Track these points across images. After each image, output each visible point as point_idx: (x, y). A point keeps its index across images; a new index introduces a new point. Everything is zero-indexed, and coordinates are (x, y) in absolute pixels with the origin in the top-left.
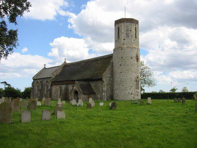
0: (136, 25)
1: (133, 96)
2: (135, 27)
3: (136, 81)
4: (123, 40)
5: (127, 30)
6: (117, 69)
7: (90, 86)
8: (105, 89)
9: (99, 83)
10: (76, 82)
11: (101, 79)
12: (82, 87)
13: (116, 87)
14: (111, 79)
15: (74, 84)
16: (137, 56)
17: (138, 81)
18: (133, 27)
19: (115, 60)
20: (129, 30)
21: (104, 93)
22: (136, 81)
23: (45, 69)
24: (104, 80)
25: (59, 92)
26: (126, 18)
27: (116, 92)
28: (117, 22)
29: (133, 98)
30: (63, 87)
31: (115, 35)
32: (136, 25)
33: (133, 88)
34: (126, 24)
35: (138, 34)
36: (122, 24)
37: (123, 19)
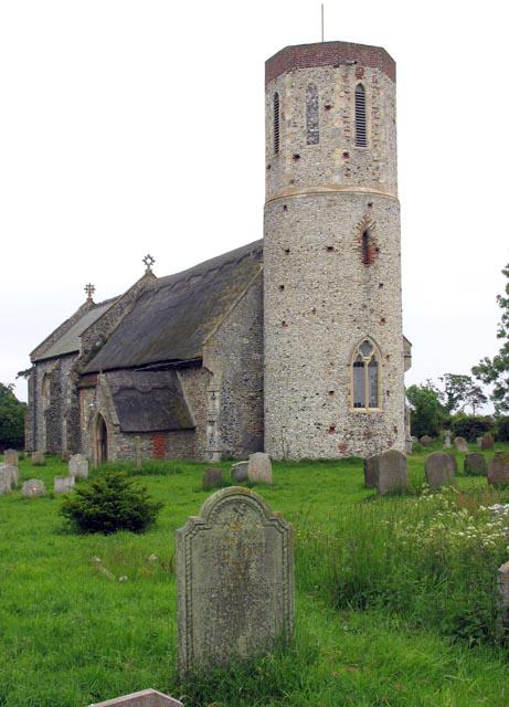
0: (359, 76)
1: (338, 438)
2: (354, 83)
3: (359, 364)
4: (289, 161)
5: (312, 108)
7: (174, 391)
9: (200, 380)
10: (102, 378)
11: (197, 364)
12: (127, 403)
14: (256, 356)
15: (94, 387)
17: (374, 364)
20: (321, 103)
21: (209, 429)
22: (359, 364)
24: (209, 363)
26: (326, 40)
27: (272, 419)
29: (343, 447)
32: (359, 76)
33: (341, 397)
34: (308, 75)
37: (338, 42)
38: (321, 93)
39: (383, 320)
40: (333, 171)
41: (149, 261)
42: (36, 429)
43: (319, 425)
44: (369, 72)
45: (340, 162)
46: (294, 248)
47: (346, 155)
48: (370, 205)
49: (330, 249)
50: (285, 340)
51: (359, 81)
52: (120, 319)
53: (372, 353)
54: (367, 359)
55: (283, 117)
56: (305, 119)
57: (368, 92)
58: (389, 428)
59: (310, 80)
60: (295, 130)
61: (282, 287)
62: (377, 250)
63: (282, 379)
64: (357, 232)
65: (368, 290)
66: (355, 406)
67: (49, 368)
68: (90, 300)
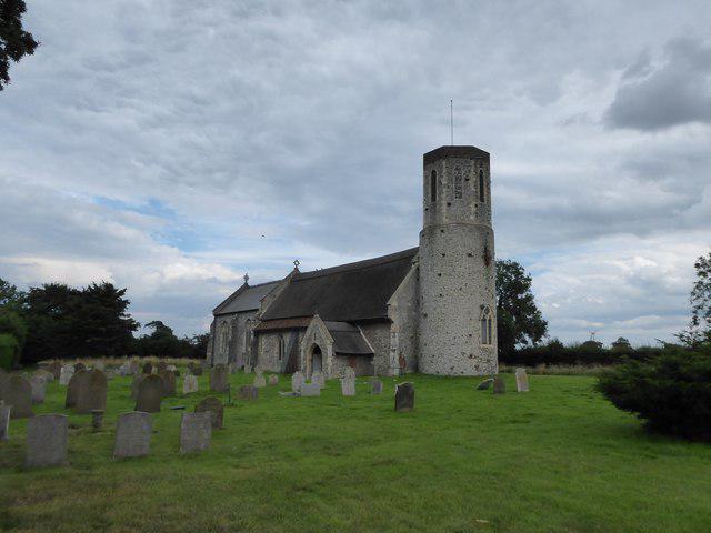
1: (474, 362)
4: (444, 207)
6: (430, 290)
8: (395, 341)
13: (424, 339)
16: (486, 250)
19: (423, 262)
21: (392, 354)
23: (246, 287)
24: (392, 315)
25: (277, 350)
28: (432, 158)
30: (287, 338)
31: (426, 194)
35: (489, 189)
36: (444, 163)
43: (463, 354)
45: (474, 209)
49: (470, 255)
67: (228, 319)
68: (246, 284)
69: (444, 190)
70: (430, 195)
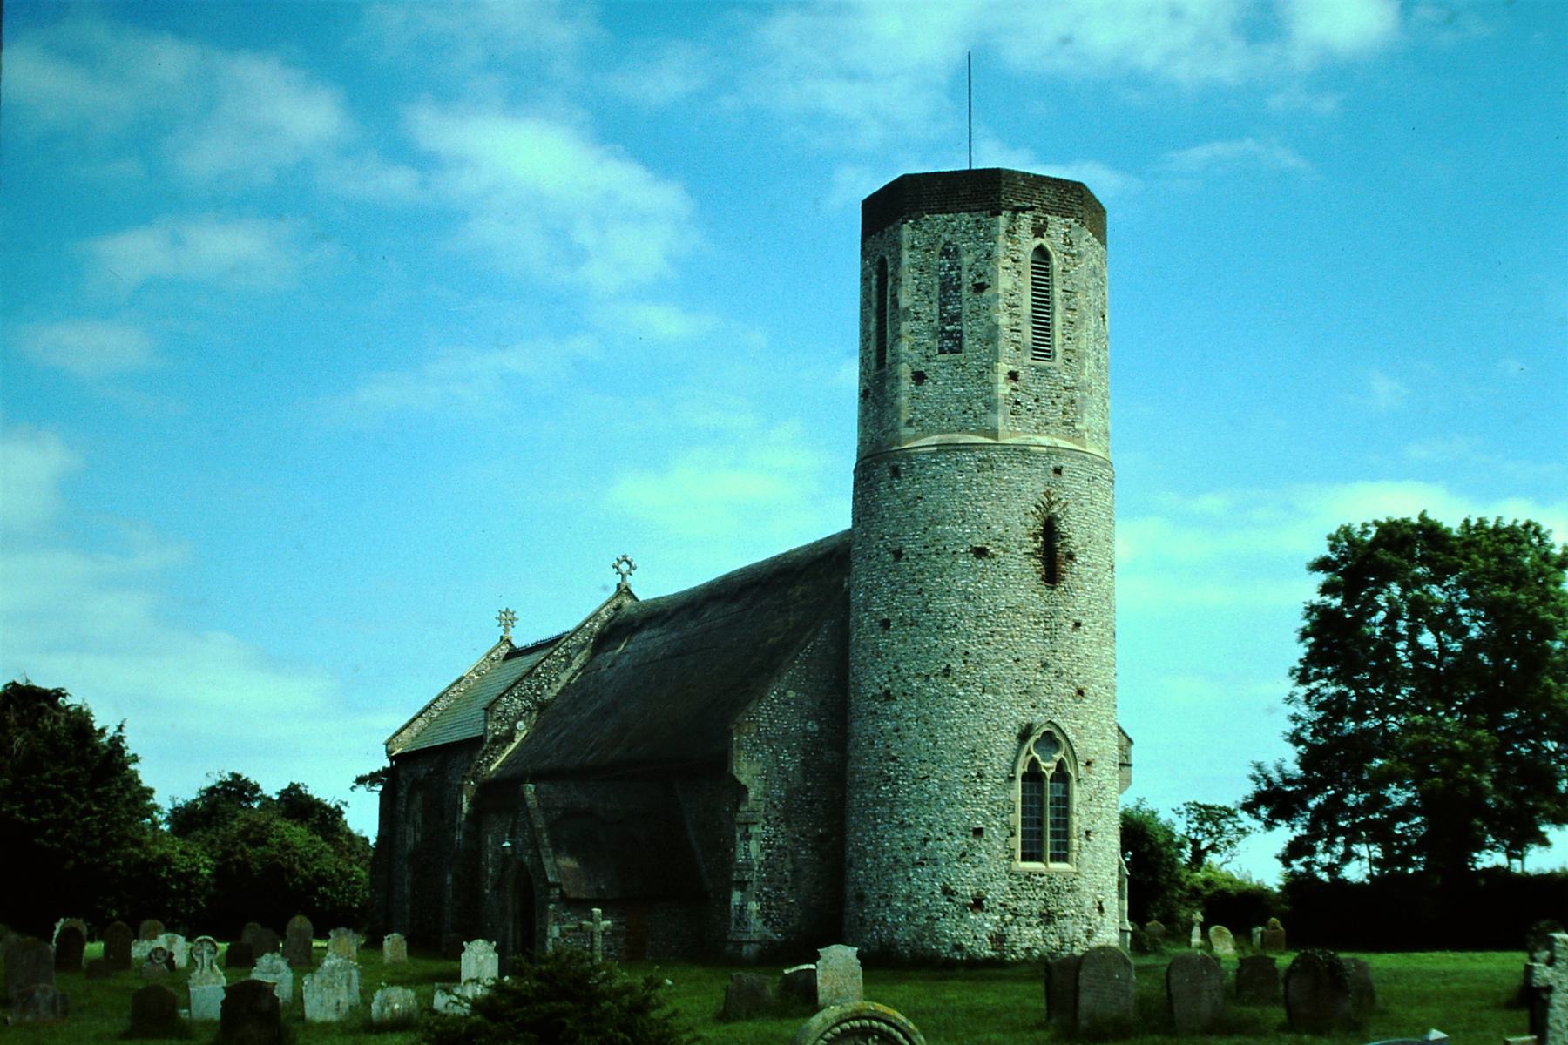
0: (1039, 231)
1: (988, 922)
2: (1029, 244)
3: (1033, 776)
4: (906, 384)
5: (949, 287)
14: (829, 755)
17: (1061, 775)
18: (1000, 252)
19: (861, 579)
20: (967, 278)
21: (736, 897)
22: (1033, 776)
31: (865, 340)
32: (1039, 231)
33: (995, 839)
38: (967, 260)
39: (1080, 692)
40: (988, 405)
41: (624, 567)
42: (531, 825)
44: (1057, 225)
46: (910, 547)
47: (1013, 376)
48: (1058, 471)
50: (889, 725)
51: (1039, 241)
52: (564, 677)
53: (1058, 756)
54: (1048, 767)
55: (895, 303)
56: (936, 310)
57: (1056, 262)
58: (1089, 903)
59: (947, 236)
60: (917, 326)
61: (886, 624)
62: (1071, 556)
63: (882, 802)
64: (1031, 520)
65: (1051, 634)
66: (1024, 859)
69: (905, 326)
70: (873, 345)
